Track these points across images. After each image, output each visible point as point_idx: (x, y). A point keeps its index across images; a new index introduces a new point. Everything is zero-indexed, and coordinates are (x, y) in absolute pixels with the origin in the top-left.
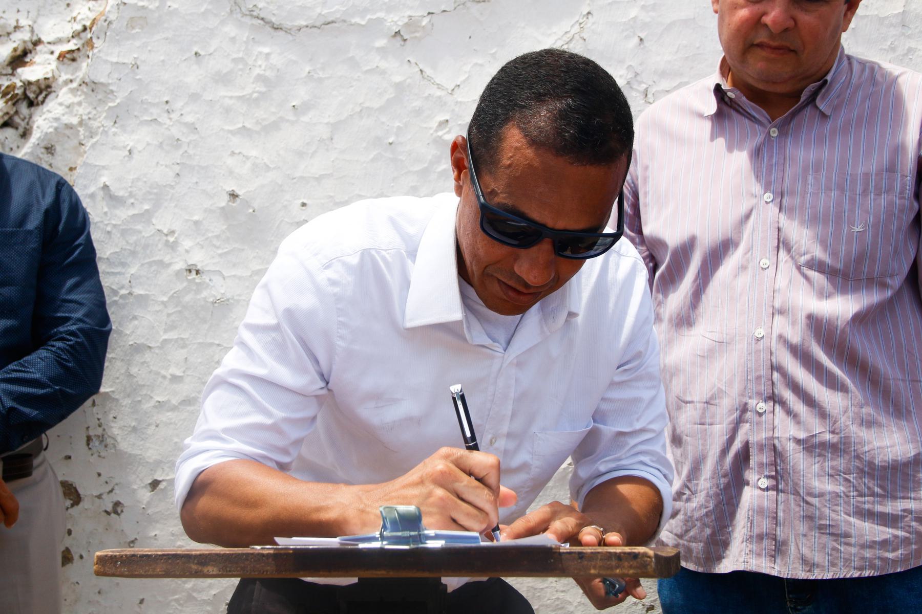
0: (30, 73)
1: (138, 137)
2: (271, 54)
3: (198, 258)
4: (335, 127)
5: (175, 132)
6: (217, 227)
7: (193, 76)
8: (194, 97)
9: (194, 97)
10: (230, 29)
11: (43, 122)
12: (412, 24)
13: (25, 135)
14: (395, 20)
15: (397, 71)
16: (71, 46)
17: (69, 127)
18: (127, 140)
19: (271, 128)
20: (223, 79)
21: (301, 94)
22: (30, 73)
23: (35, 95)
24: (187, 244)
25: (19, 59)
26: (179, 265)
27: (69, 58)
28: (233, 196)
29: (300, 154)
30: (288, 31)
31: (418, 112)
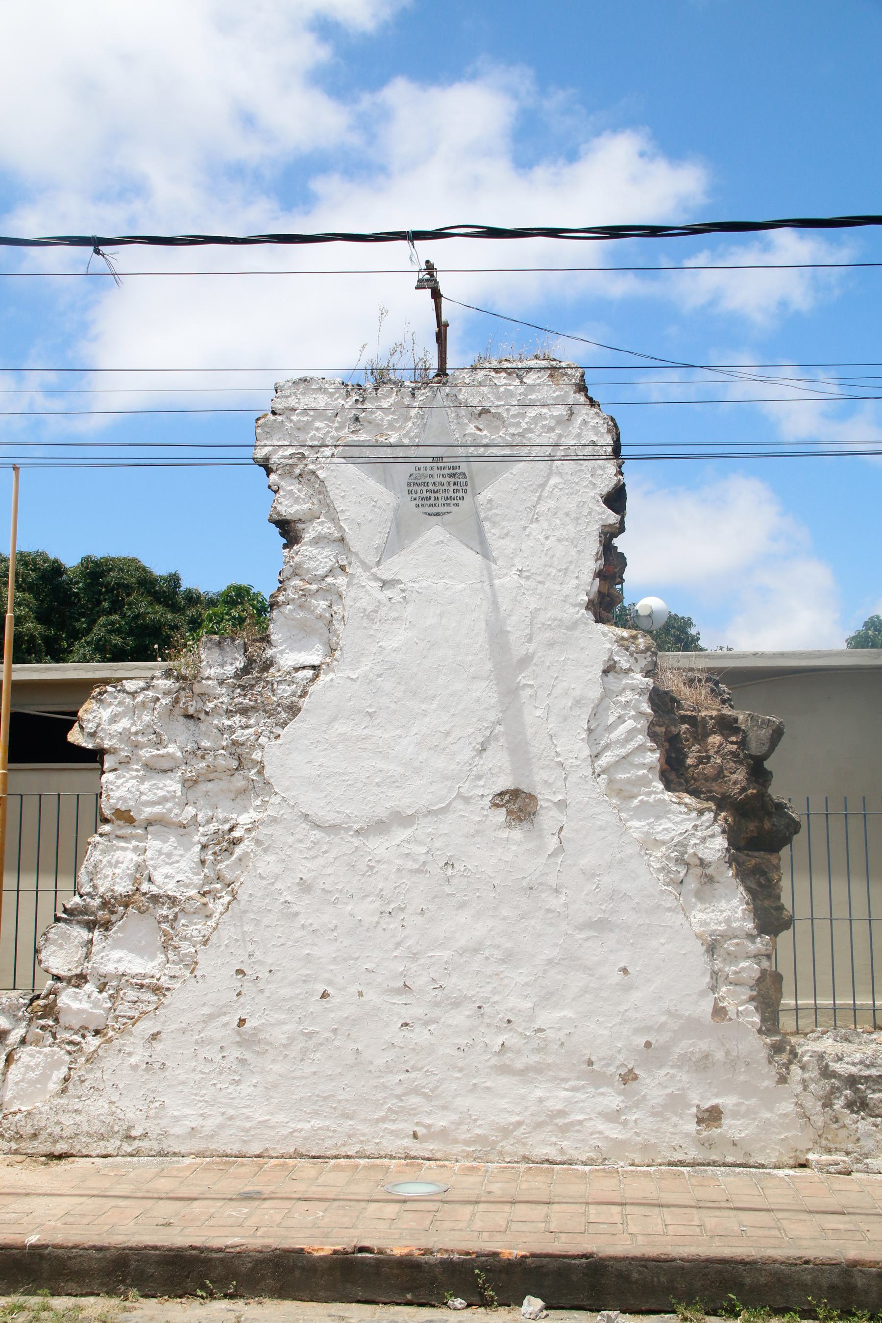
0: (236, 834)
1: (271, 858)
2: (316, 834)
3: (289, 898)
4: (335, 858)
5: (283, 857)
6: (296, 888)
7: (290, 840)
8: (291, 846)
9: (291, 846)
10: (303, 825)
11: (238, 851)
12: (362, 828)
13: (232, 854)
14: (356, 827)
15: (356, 841)
16: (250, 826)
17: (247, 852)
18: (267, 858)
19: (316, 857)
20: (300, 841)
21: (325, 848)
22: (236, 834)
23: (235, 842)
24: (285, 893)
25: (231, 829)
26: (282, 900)
27: (249, 830)
28: (301, 879)
29: (324, 867)
30: (322, 827)
31: (362, 856)
